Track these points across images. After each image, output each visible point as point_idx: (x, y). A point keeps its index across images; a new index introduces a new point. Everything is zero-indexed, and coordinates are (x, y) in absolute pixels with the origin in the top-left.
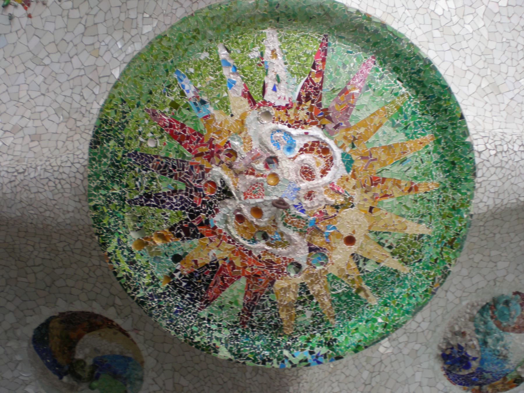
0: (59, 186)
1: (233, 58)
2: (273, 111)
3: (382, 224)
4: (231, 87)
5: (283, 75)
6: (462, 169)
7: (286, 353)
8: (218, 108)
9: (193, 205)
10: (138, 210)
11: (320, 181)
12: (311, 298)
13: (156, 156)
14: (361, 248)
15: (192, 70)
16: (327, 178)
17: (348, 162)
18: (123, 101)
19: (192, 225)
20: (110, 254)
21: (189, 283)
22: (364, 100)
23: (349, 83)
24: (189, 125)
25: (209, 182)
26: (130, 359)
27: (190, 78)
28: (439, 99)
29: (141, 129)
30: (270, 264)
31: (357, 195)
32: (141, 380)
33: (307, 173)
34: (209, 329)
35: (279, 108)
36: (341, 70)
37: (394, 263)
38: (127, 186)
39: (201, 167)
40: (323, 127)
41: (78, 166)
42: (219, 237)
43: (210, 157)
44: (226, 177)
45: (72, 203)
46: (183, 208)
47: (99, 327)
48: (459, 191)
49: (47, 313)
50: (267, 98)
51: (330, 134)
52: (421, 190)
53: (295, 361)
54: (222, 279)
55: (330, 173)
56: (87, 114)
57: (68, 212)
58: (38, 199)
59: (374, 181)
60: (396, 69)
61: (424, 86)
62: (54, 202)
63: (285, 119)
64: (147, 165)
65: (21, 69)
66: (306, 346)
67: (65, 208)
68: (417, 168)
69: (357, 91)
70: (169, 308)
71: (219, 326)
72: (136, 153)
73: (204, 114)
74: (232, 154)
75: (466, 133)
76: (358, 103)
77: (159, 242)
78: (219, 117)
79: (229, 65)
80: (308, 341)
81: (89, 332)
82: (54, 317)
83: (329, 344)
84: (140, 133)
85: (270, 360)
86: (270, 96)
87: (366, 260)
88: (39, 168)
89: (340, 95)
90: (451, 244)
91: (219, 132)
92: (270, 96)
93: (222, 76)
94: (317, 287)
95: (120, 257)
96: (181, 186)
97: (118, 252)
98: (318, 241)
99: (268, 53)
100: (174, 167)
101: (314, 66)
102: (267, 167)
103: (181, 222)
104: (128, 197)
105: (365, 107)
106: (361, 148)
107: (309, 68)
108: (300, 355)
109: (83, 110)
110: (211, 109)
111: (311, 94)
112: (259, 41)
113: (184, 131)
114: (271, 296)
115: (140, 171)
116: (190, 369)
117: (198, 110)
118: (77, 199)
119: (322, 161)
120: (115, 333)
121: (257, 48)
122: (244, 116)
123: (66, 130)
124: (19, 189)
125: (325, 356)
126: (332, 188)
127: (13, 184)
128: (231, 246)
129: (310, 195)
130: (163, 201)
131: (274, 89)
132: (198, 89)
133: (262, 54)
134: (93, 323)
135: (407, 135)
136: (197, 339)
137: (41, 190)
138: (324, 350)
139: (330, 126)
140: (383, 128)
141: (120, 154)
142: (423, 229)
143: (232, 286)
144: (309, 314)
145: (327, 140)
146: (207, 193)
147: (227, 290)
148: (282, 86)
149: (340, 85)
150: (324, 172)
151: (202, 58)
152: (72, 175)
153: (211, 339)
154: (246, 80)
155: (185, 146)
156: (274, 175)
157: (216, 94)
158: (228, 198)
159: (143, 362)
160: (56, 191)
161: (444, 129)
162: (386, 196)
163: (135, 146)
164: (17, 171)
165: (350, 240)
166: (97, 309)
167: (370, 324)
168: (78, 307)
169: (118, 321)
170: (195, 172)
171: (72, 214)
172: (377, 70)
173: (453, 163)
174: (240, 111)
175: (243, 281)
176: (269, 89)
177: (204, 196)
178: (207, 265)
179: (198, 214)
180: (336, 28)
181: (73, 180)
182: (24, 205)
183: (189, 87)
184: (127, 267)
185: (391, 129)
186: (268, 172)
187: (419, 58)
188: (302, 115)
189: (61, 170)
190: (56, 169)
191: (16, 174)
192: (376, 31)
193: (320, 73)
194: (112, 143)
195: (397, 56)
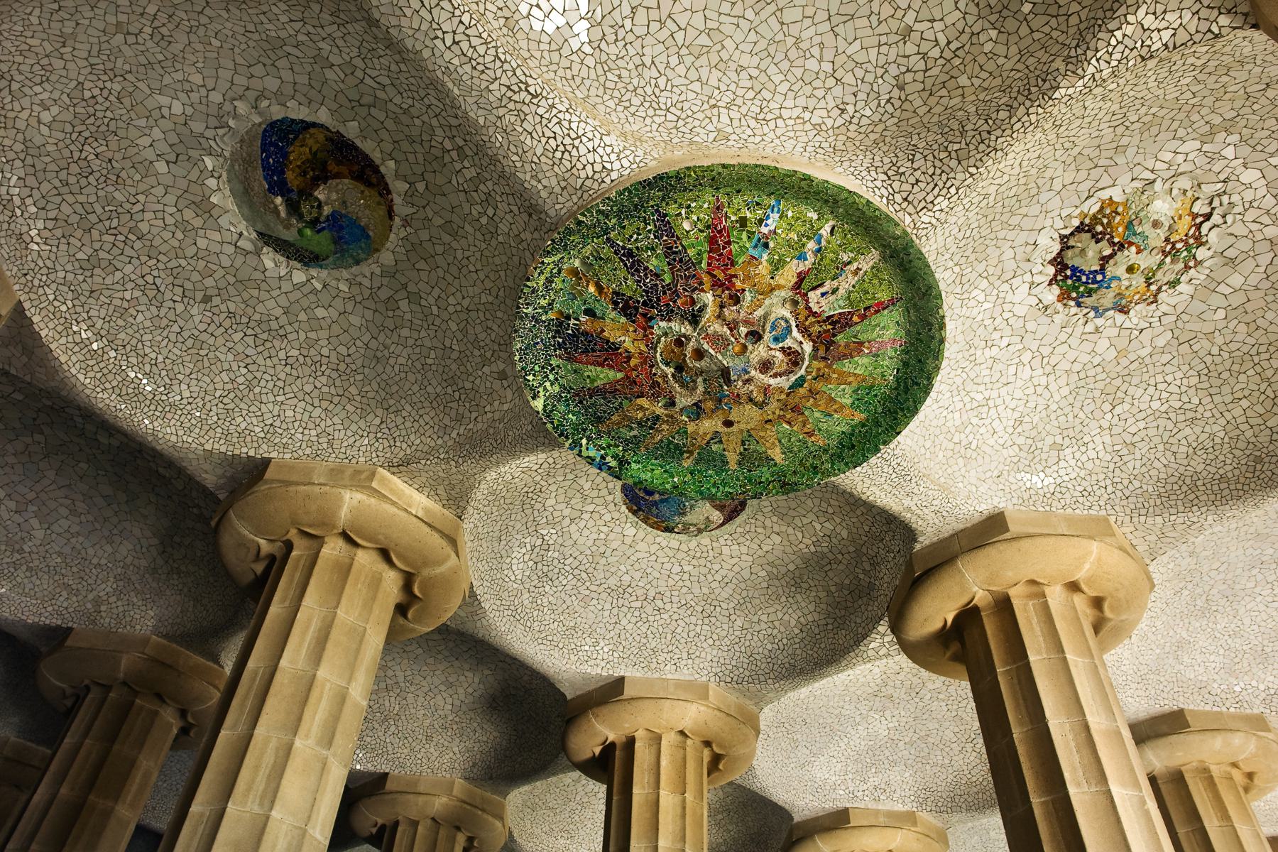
0: (558, 155)
1: (829, 242)
2: (802, 306)
3: (762, 434)
4: (799, 258)
5: (841, 292)
6: (853, 455)
7: (584, 441)
8: (770, 262)
9: (658, 299)
10: (607, 251)
12: (651, 428)
13: (678, 238)
14: (728, 434)
17: (800, 383)
19: (636, 309)
20: (543, 263)
21: (574, 335)
24: (734, 247)
25: (692, 299)
26: (368, 237)
27: (781, 218)
28: (902, 410)
29: (693, 205)
31: (773, 406)
32: (357, 263)
34: (547, 376)
37: (732, 458)
38: (624, 227)
39: (701, 283)
40: (815, 349)
41: (598, 159)
42: (645, 336)
43: (717, 284)
44: (709, 310)
45: (554, 182)
46: (647, 292)
47: (369, 185)
48: (833, 464)
49: (323, 116)
50: (811, 294)
53: (585, 453)
54: (606, 360)
56: (621, 44)
57: (540, 181)
58: (522, 138)
59: (796, 409)
60: (906, 364)
61: (906, 393)
62: (535, 159)
63: (801, 318)
64: (662, 236)
67: (540, 176)
71: (556, 379)
72: (665, 215)
73: (755, 253)
74: (736, 300)
75: (885, 443)
77: (592, 289)
78: (764, 268)
79: (819, 243)
80: (609, 446)
81: (353, 178)
82: (327, 129)
83: (622, 462)
84: (689, 207)
85: (567, 438)
86: (814, 296)
87: (721, 442)
88: (554, 111)
90: (784, 484)
91: (748, 277)
92: (814, 296)
93: (804, 245)
94: (665, 427)
96: (667, 279)
97: (551, 266)
100: (681, 261)
102: (746, 335)
103: (631, 298)
104: (612, 235)
106: (820, 386)
107: (862, 306)
108: (592, 453)
109: (621, 33)
110: (765, 256)
111: (840, 323)
112: (859, 252)
113: (724, 248)
114: (625, 402)
115: (650, 231)
116: (423, 303)
117: (756, 246)
118: (563, 184)
119: (784, 367)
120: (379, 204)
121: (852, 255)
122: (779, 287)
123: (584, 38)
124: (511, 106)
125: (610, 468)
127: (509, 94)
128: (643, 348)
130: (637, 270)
131: (823, 295)
132: (775, 232)
133: (850, 263)
134: (366, 173)
136: (530, 378)
137: (534, 134)
138: (613, 463)
139: (821, 353)
141: (651, 203)
142: (777, 455)
143: (606, 370)
146: (679, 302)
147: (599, 369)
148: (832, 298)
149: (862, 337)
150: (775, 376)
151: (809, 215)
152: (583, 160)
153: (540, 385)
154: (816, 268)
155: (710, 258)
156: (745, 348)
157: (782, 251)
158: (691, 324)
159: (377, 250)
160: (551, 155)
161: (878, 424)
163: (672, 209)
164: (527, 85)
166: (388, 168)
167: (665, 475)
168: (367, 146)
169: (397, 200)
170: (691, 282)
171: (540, 187)
173: (853, 446)
174: (782, 282)
175: (620, 375)
177: (675, 302)
178: (608, 341)
179: (653, 307)
180: (915, 304)
181: (579, 166)
182: (499, 124)
183: (773, 221)
184: (541, 283)
186: (743, 341)
187: (930, 379)
189: (577, 142)
190: (573, 135)
191: (523, 86)
192: (933, 338)
195: (920, 361)
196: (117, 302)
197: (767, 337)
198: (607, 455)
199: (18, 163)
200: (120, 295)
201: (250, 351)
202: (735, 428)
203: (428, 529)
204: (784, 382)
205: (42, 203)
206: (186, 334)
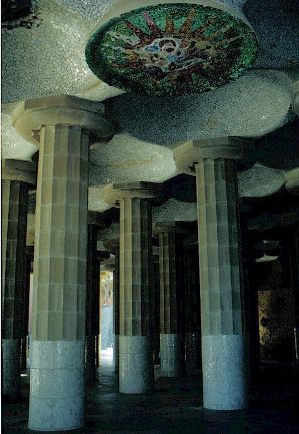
2: (139, 46)
5: (128, 38)
7: (231, 76)
11: (176, 49)
15: (106, 54)
16: (177, 46)
22: (158, 23)
23: (147, 24)
24: (124, 63)
33: (169, 50)
35: (139, 44)
37: (232, 39)
51: (162, 37)
55: (176, 43)
66: (236, 70)
69: (153, 23)
76: (158, 25)
83: (242, 66)
86: (132, 44)
89: (149, 28)
99: (116, 37)
101: (132, 29)
105: (162, 24)
111: (141, 35)
112: (109, 35)
121: (112, 38)
126: (182, 46)
129: (179, 53)
133: (115, 38)
135: (184, 17)
140: (174, 23)
145: (163, 39)
148: (132, 40)
149: (146, 26)
150: (175, 45)
165: (208, 48)
172: (150, 13)
176: (129, 43)
185: (177, 21)
186: (159, 59)
188: (147, 40)
193: (136, 29)
197: (156, 52)
198: (238, 70)
201: (259, 88)
204: (178, 42)
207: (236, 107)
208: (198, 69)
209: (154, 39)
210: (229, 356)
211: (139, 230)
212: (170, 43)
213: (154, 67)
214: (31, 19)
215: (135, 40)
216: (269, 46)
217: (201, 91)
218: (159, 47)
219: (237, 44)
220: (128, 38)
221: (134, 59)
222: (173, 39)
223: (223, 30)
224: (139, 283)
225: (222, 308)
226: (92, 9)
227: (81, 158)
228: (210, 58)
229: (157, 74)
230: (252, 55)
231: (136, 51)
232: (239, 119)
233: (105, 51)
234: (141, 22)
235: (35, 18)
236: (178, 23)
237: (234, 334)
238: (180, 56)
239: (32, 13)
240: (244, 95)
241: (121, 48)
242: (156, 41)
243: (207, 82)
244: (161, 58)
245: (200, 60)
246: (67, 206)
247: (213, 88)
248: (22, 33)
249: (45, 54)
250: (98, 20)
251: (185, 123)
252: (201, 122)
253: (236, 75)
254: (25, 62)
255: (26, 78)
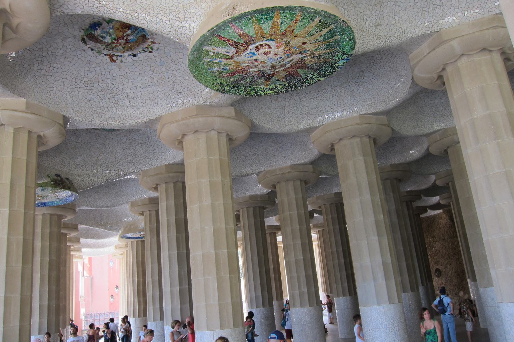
7: (337, 65)
11: (273, 50)
16: (273, 48)
18: (213, 84)
22: (247, 31)
24: (229, 72)
30: (296, 64)
33: (266, 53)
35: (236, 53)
36: (230, 34)
37: (325, 31)
51: (255, 43)
52: (299, 18)
59: (284, 33)
65: (182, 54)
68: (287, 19)
69: (242, 32)
70: (295, 85)
83: (344, 53)
92: (230, 55)
95: (267, 92)
97: (265, 92)
98: (298, 52)
99: (213, 51)
101: (225, 41)
105: (250, 30)
111: (236, 45)
122: (234, 61)
129: (276, 55)
136: (311, 83)
144: (327, 55)
148: (228, 51)
149: (237, 36)
150: (270, 47)
162: (293, 31)
165: (304, 43)
176: (227, 54)
184: (272, 91)
186: (260, 63)
188: (243, 48)
193: (229, 40)
194: (226, 88)
196: (364, 92)
197: (255, 57)
199: (321, 109)
200: (361, 91)
202: (306, 40)
203: (433, 53)
204: (272, 44)
205: (333, 105)
206: (374, 78)
207: (361, 86)
208: (301, 64)
209: (248, 46)
210: (388, 326)
211: (296, 209)
212: (265, 47)
213: (258, 71)
214: (150, 44)
215: (231, 51)
216: (374, 26)
217: (311, 83)
218: (256, 53)
219: (331, 34)
220: (224, 49)
221: (237, 68)
222: (266, 42)
223: (314, 24)
224: (301, 258)
225: (375, 279)
226: (184, 30)
227: (220, 159)
228: (309, 52)
229: (264, 76)
230: (351, 42)
231: (235, 59)
232: (367, 97)
233: (209, 65)
234: (231, 33)
235: (153, 42)
236: (266, 27)
237: (390, 304)
238: (278, 57)
239: (149, 39)
240: (366, 75)
241: (221, 60)
242: (251, 47)
243: (315, 74)
244: (261, 62)
245: (299, 56)
246: (212, 203)
247: (322, 79)
248: (146, 58)
249: (170, 72)
250: (192, 39)
251: (317, 109)
252: (330, 106)
253: (341, 63)
254: (156, 82)
255: (160, 96)
